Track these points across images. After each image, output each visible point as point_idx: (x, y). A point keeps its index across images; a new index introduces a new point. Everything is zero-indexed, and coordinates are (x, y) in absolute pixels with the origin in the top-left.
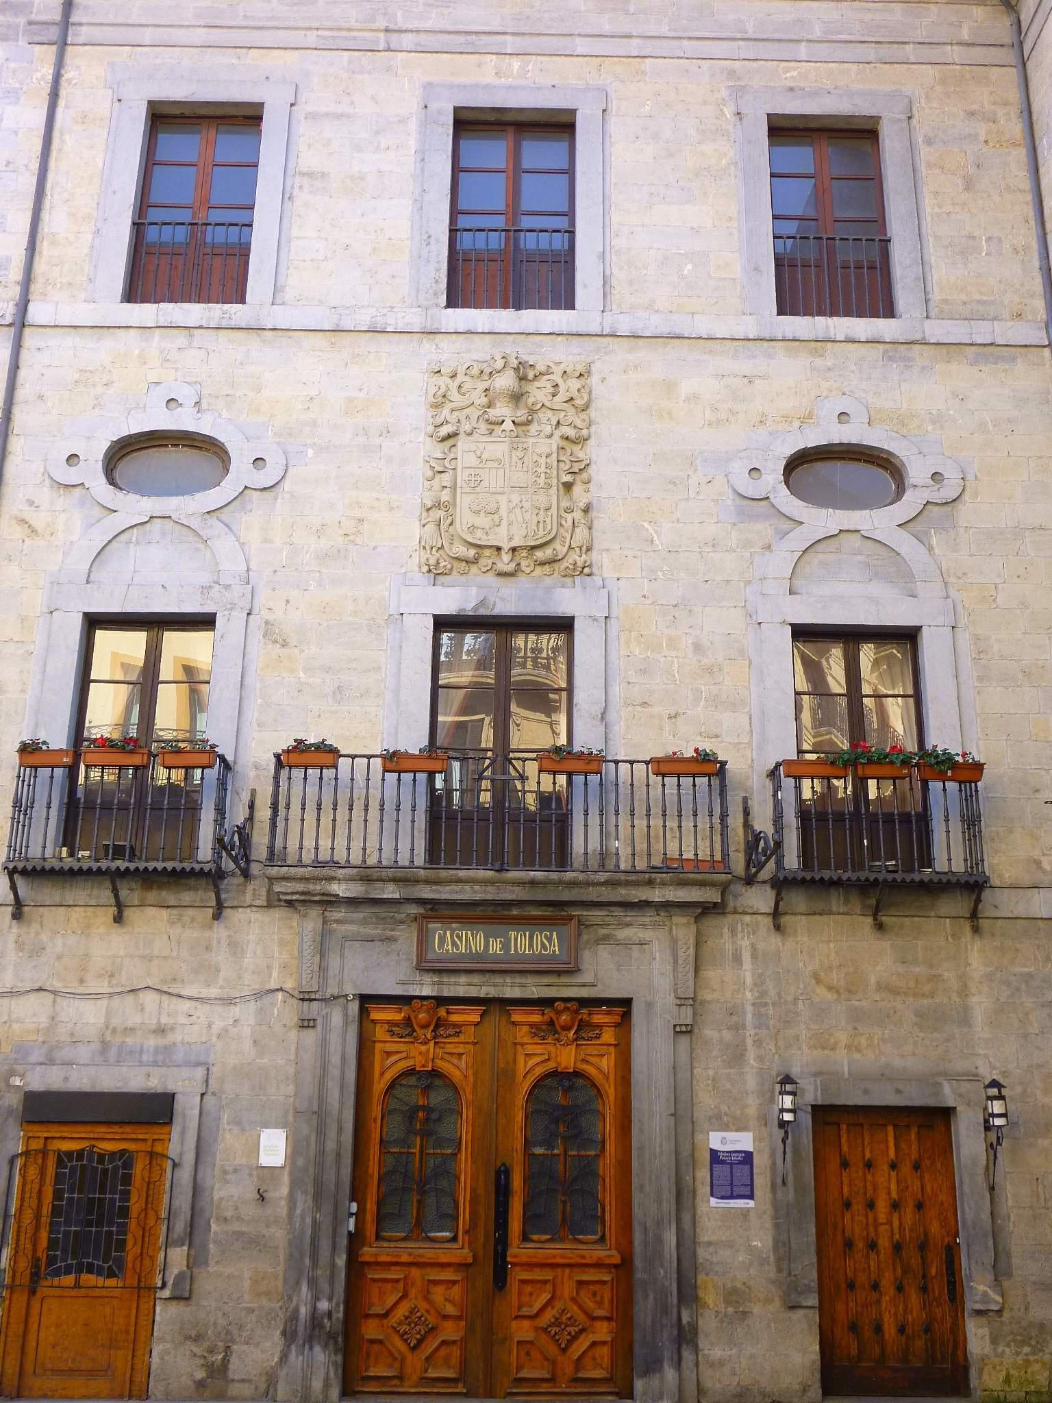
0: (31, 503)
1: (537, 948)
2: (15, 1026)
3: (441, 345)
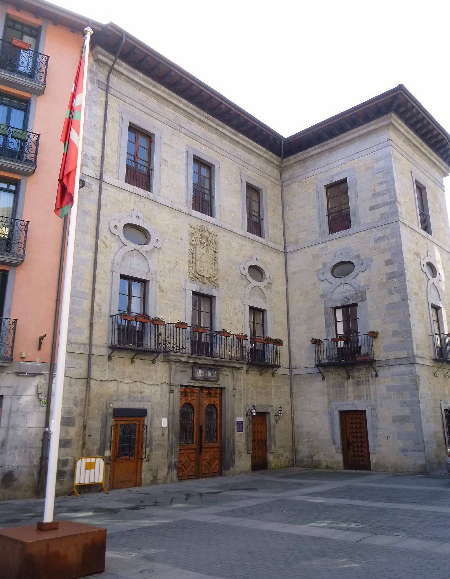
0: (105, 237)
2: (109, 390)
3: (191, 219)
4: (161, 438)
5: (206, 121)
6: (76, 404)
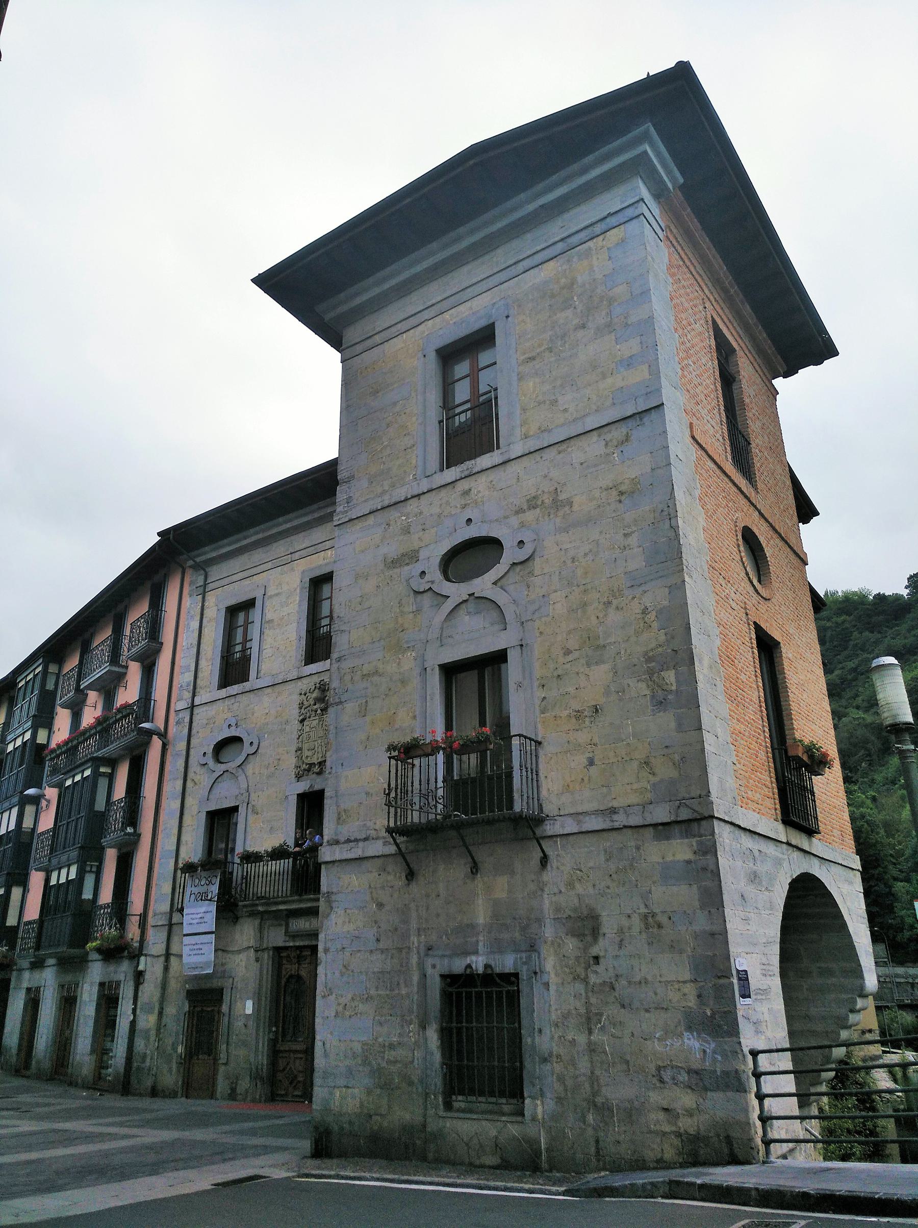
4: (244, 1030)
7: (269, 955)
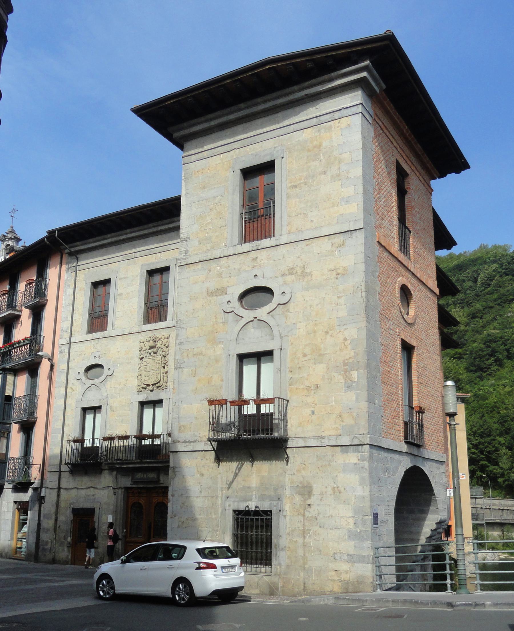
1: (152, 476)
5: (155, 229)
6: (53, 506)
7: (122, 492)
